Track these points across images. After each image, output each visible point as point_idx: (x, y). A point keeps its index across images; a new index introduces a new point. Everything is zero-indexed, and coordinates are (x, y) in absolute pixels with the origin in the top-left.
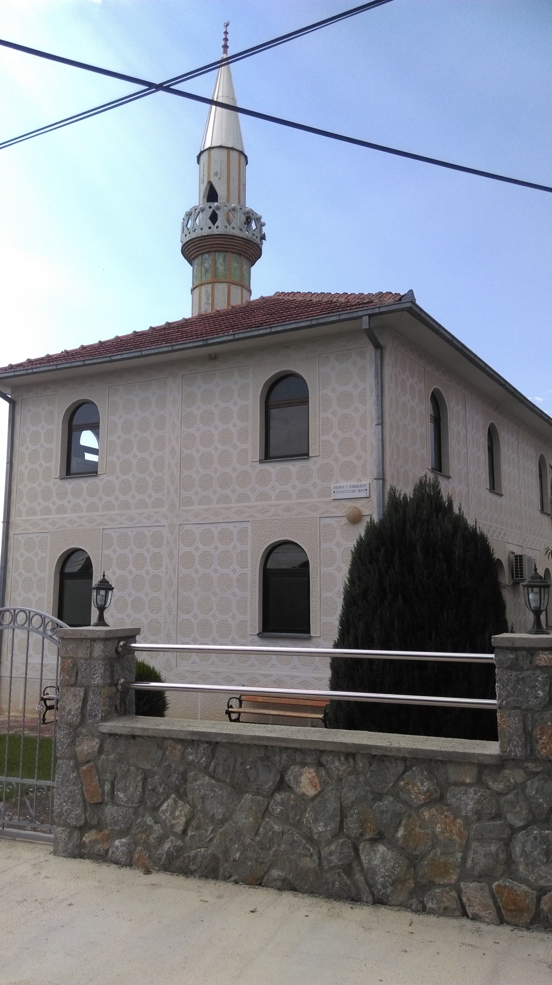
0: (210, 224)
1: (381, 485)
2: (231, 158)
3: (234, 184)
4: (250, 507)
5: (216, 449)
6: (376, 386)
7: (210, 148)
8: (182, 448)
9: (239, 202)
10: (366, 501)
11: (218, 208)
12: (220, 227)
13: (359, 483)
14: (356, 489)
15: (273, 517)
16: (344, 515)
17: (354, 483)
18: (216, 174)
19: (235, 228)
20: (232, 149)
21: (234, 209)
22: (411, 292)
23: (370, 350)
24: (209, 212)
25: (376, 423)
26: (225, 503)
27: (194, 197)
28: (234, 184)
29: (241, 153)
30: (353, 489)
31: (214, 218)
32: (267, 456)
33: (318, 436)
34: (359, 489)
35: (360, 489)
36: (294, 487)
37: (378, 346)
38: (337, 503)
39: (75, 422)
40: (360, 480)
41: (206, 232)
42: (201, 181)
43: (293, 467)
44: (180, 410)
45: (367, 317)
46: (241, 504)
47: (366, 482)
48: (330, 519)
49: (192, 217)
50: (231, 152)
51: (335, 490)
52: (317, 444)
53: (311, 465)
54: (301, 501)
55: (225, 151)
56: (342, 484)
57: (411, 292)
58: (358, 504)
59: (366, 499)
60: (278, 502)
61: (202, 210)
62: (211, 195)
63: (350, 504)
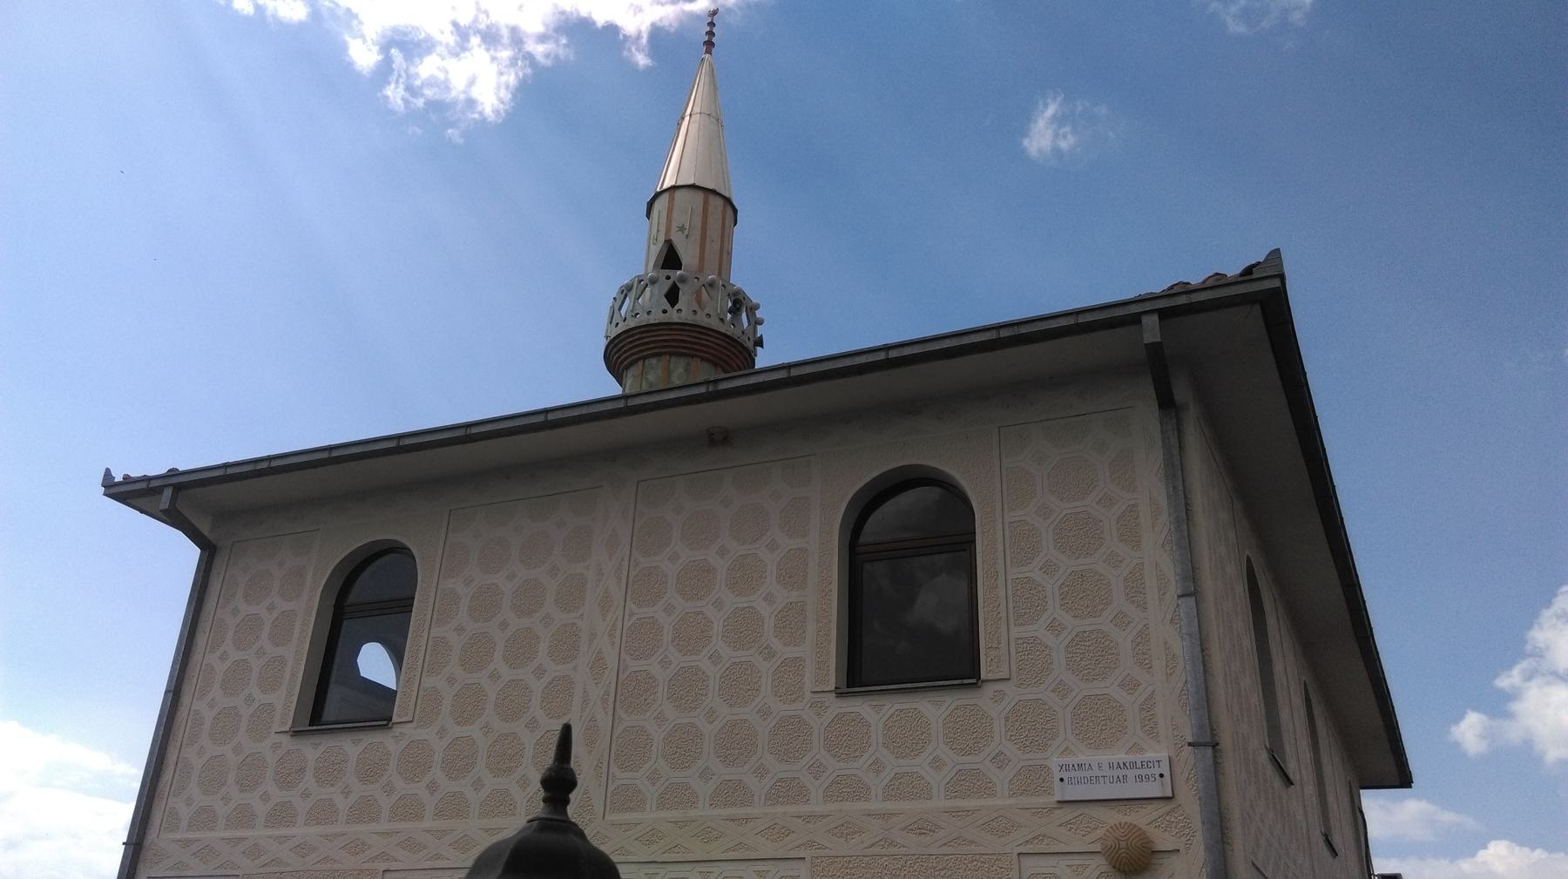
0: (667, 306)
1: (1210, 761)
2: (710, 209)
3: (713, 248)
4: (808, 818)
5: (715, 658)
6: (1169, 497)
7: (674, 188)
8: (623, 655)
9: (720, 274)
10: (1165, 808)
11: (683, 280)
12: (683, 312)
13: (1138, 758)
14: (1131, 774)
15: (876, 850)
16: (1097, 847)
17: (1122, 757)
18: (682, 229)
19: (713, 314)
20: (714, 192)
21: (712, 284)
22: (1275, 255)
23: (1145, 412)
24: (667, 285)
25: (1179, 592)
26: (734, 804)
27: (639, 260)
28: (713, 248)
29: (728, 201)
30: (1121, 773)
31: (672, 296)
32: (860, 673)
33: (1004, 628)
34: (1138, 772)
35: (1144, 772)
36: (937, 764)
37: (1167, 403)
38: (1067, 814)
39: (354, 596)
40: (1136, 748)
41: (656, 317)
42: (652, 240)
43: (934, 709)
44: (626, 563)
45: (1155, 318)
46: (780, 809)
47: (1158, 753)
48: (1052, 860)
49: (633, 293)
50: (712, 198)
51: (1065, 775)
52: (1003, 645)
53: (989, 703)
54: (959, 803)
55: (700, 196)
56: (1082, 758)
57: (1275, 255)
58: (1141, 818)
59: (1162, 803)
60: (890, 806)
61: (653, 281)
62: (670, 259)
63: (1113, 817)
